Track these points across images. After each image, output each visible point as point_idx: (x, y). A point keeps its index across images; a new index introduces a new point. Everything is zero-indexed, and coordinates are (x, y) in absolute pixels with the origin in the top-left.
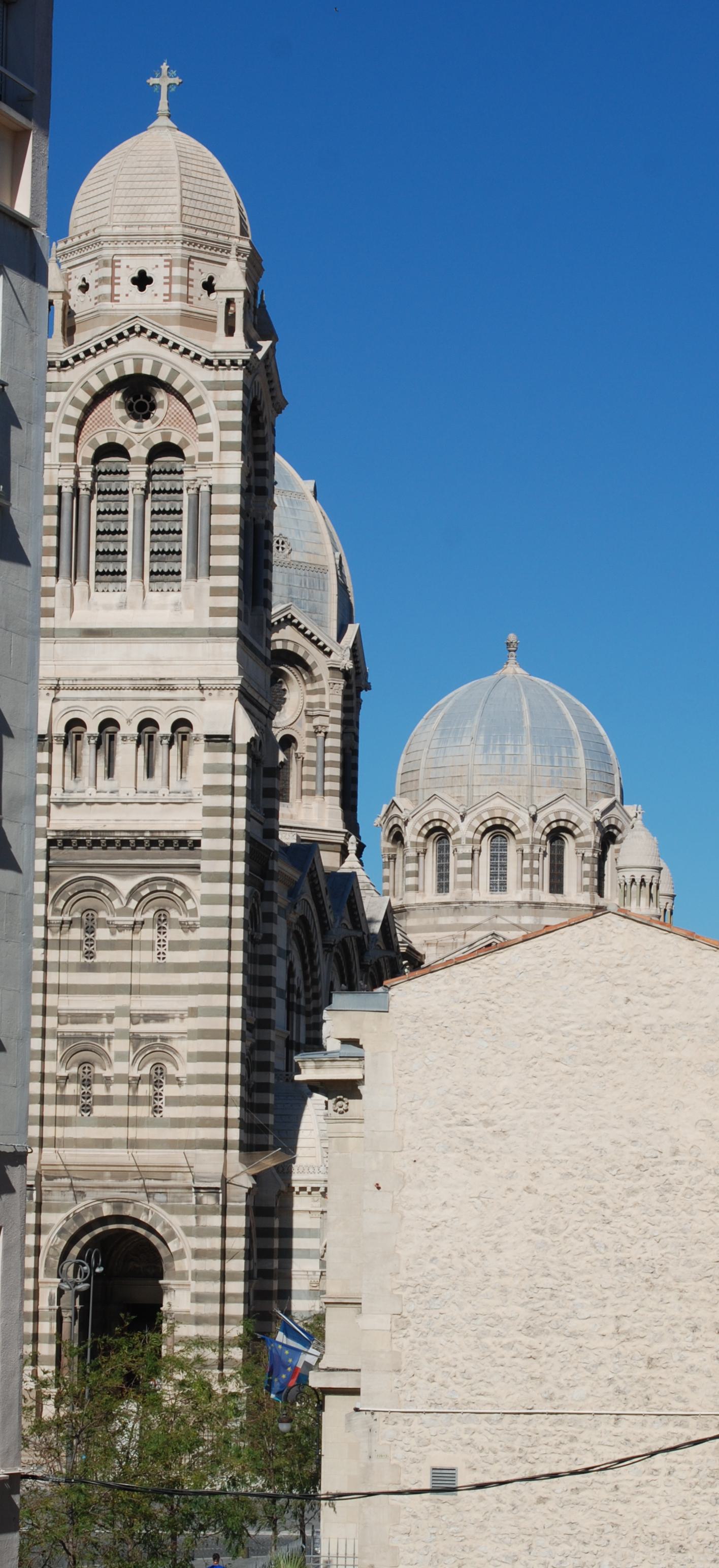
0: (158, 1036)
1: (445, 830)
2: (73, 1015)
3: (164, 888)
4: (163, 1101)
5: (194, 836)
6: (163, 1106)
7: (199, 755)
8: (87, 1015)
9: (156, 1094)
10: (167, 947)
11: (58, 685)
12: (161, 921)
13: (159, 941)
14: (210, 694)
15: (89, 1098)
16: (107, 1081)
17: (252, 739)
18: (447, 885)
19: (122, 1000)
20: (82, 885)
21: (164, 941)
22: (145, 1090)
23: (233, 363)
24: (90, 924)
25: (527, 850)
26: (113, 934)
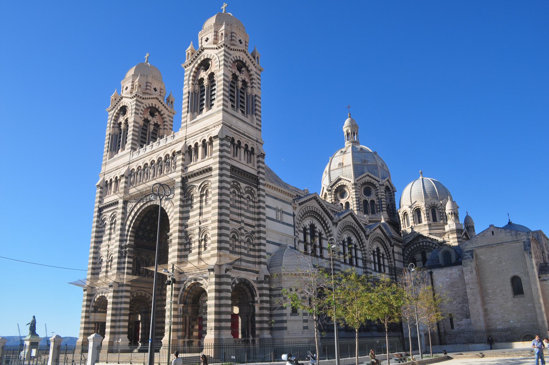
3: (207, 183)
23: (222, 46)
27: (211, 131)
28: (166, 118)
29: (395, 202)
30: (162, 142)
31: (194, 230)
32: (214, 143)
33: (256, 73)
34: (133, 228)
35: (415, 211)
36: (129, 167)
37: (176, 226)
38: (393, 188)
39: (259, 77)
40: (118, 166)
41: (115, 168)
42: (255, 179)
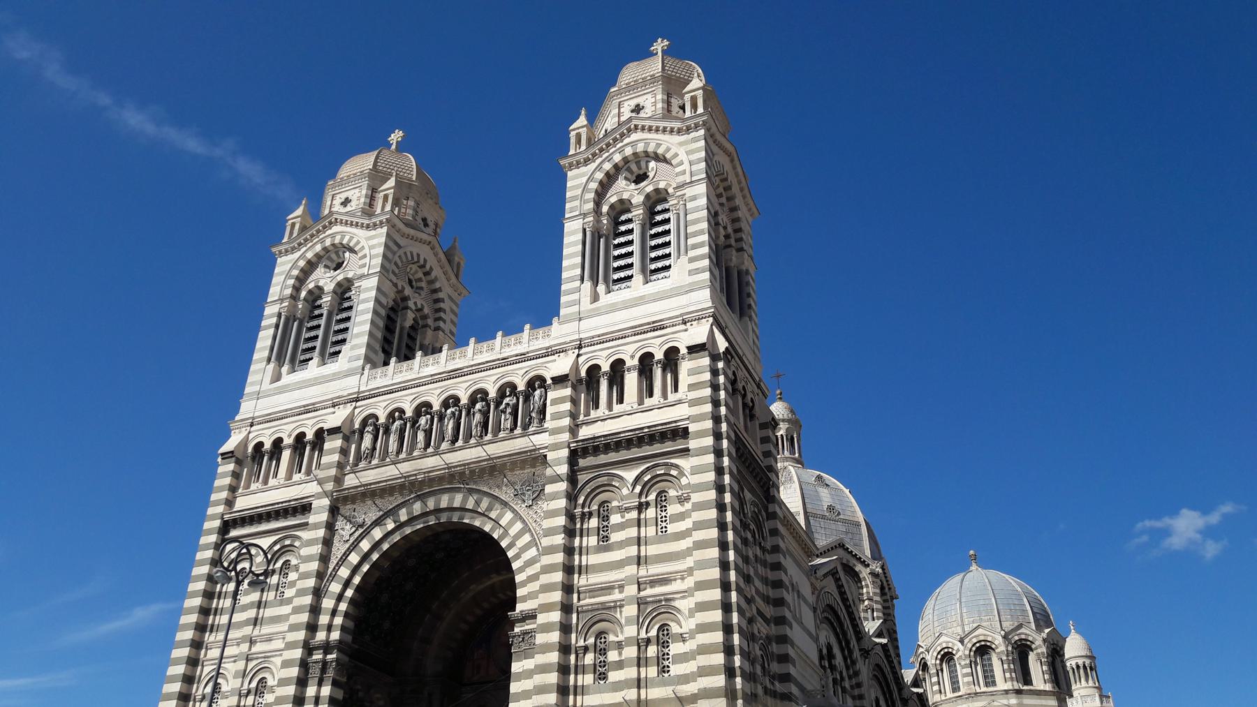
0: (662, 598)
1: (951, 653)
2: (591, 591)
3: (662, 472)
4: (670, 660)
5: (682, 424)
6: (670, 665)
7: (685, 366)
8: (602, 589)
9: (664, 655)
10: (668, 521)
11: (580, 344)
12: (662, 499)
13: (662, 518)
14: (691, 325)
15: (604, 666)
16: (619, 646)
17: (727, 348)
18: (959, 688)
19: (631, 570)
20: (598, 482)
21: (666, 517)
22: (652, 651)
23: (697, 126)
24: (606, 513)
25: (1004, 658)
26: (623, 517)
27: (673, 333)
28: (442, 300)
29: (895, 624)
30: (444, 361)
31: (615, 607)
32: (327, 446)
33: (450, 297)
34: (358, 589)
35: (975, 652)
36: (355, 408)
37: (298, 630)
38: (890, 589)
39: (454, 307)
40: (313, 404)
41: (300, 407)
42: (764, 484)
